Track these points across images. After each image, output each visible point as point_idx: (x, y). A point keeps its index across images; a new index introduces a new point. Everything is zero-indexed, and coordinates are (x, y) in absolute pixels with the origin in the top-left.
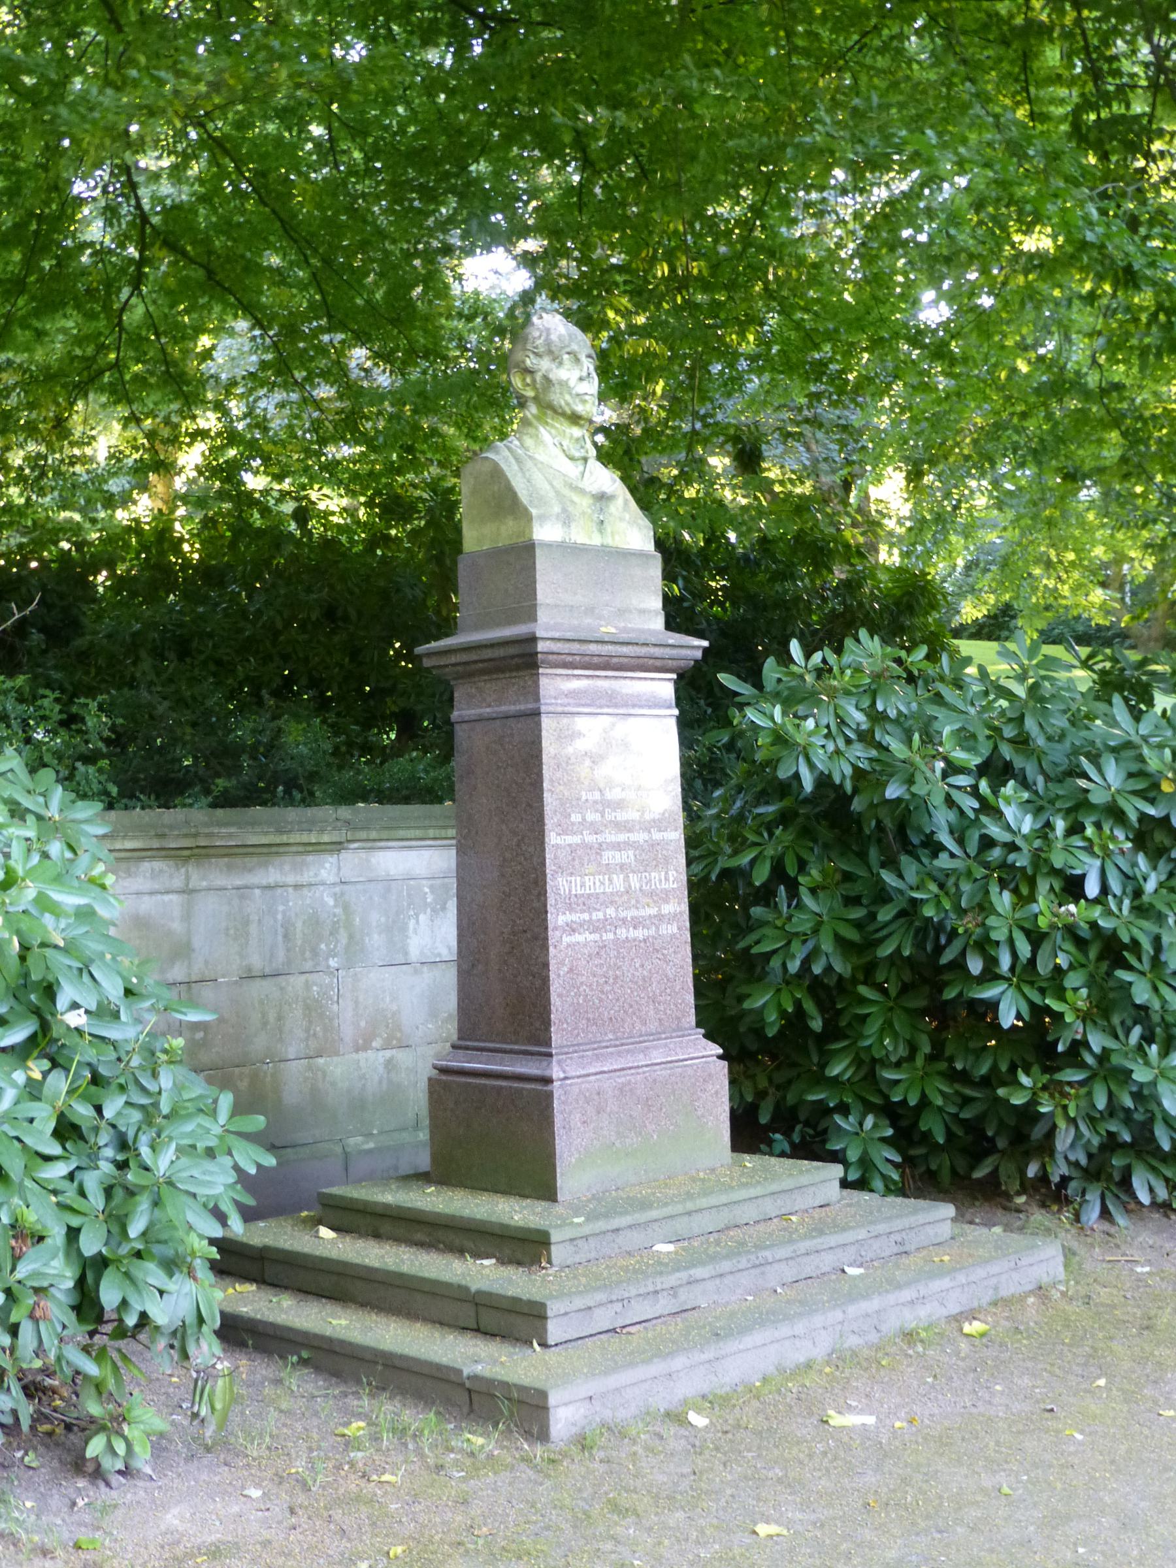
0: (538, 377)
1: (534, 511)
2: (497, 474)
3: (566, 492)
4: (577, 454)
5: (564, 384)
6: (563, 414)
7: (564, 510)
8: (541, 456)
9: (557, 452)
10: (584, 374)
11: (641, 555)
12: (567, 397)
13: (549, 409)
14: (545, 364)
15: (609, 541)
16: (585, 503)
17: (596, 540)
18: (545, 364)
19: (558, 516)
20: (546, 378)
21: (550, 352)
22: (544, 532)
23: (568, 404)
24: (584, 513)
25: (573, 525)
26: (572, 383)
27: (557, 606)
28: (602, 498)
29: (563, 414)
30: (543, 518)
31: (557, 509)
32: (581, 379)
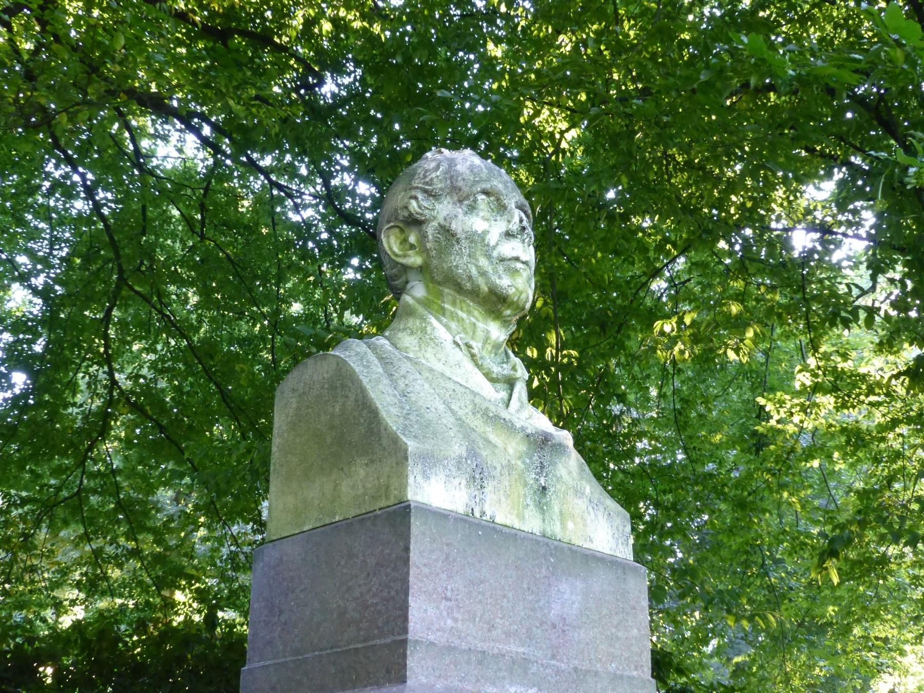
0: (430, 229)
1: (412, 445)
2: (345, 382)
3: (476, 423)
4: (496, 369)
5: (477, 239)
6: (474, 294)
7: (473, 453)
8: (430, 359)
9: (460, 356)
10: (515, 227)
11: (610, 563)
12: (483, 262)
13: (451, 285)
14: (444, 209)
15: (555, 529)
16: (514, 448)
17: (532, 524)
18: (444, 209)
19: (459, 463)
20: (446, 232)
21: (454, 189)
22: (433, 490)
23: (483, 274)
24: (510, 467)
25: (489, 487)
26: (492, 238)
27: (451, 649)
28: (542, 442)
29: (474, 294)
30: (430, 461)
31: (458, 449)
32: (508, 235)
